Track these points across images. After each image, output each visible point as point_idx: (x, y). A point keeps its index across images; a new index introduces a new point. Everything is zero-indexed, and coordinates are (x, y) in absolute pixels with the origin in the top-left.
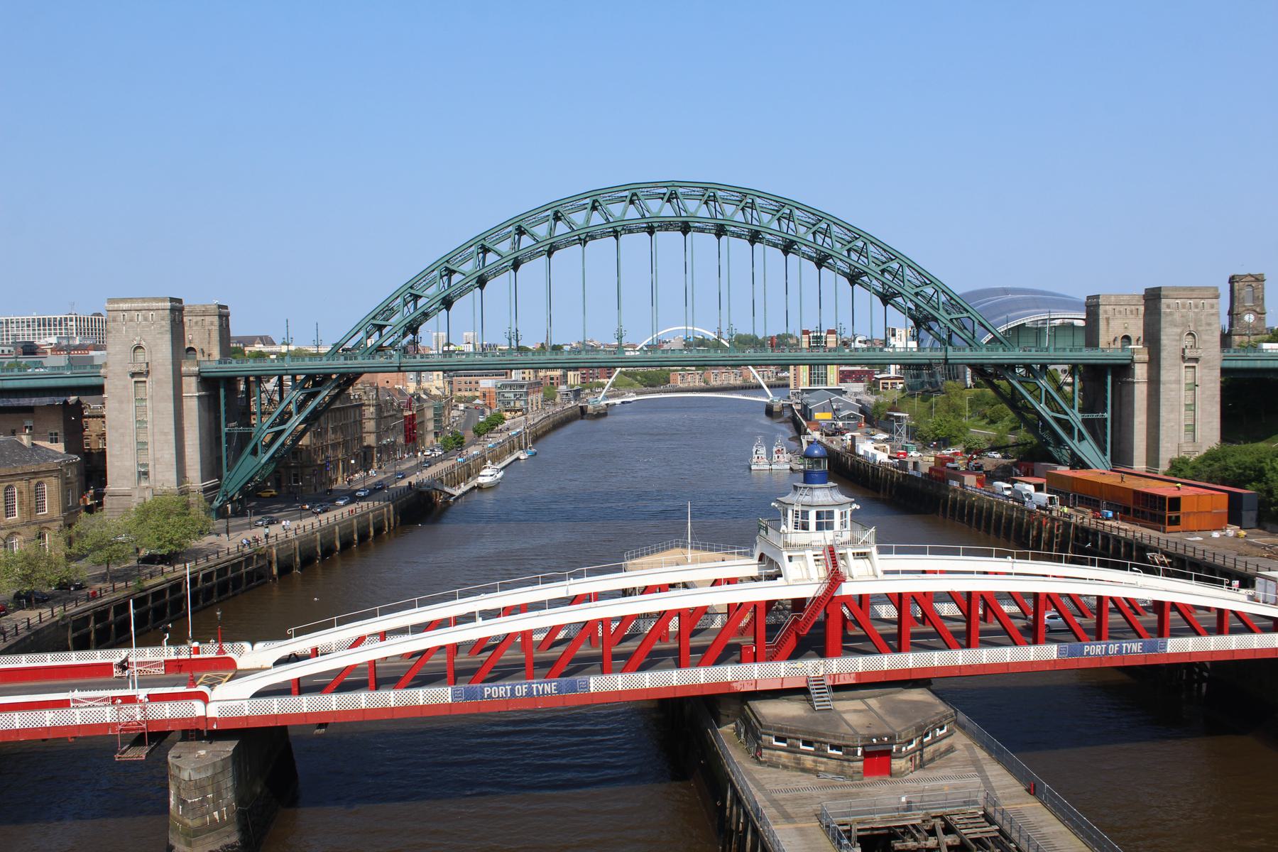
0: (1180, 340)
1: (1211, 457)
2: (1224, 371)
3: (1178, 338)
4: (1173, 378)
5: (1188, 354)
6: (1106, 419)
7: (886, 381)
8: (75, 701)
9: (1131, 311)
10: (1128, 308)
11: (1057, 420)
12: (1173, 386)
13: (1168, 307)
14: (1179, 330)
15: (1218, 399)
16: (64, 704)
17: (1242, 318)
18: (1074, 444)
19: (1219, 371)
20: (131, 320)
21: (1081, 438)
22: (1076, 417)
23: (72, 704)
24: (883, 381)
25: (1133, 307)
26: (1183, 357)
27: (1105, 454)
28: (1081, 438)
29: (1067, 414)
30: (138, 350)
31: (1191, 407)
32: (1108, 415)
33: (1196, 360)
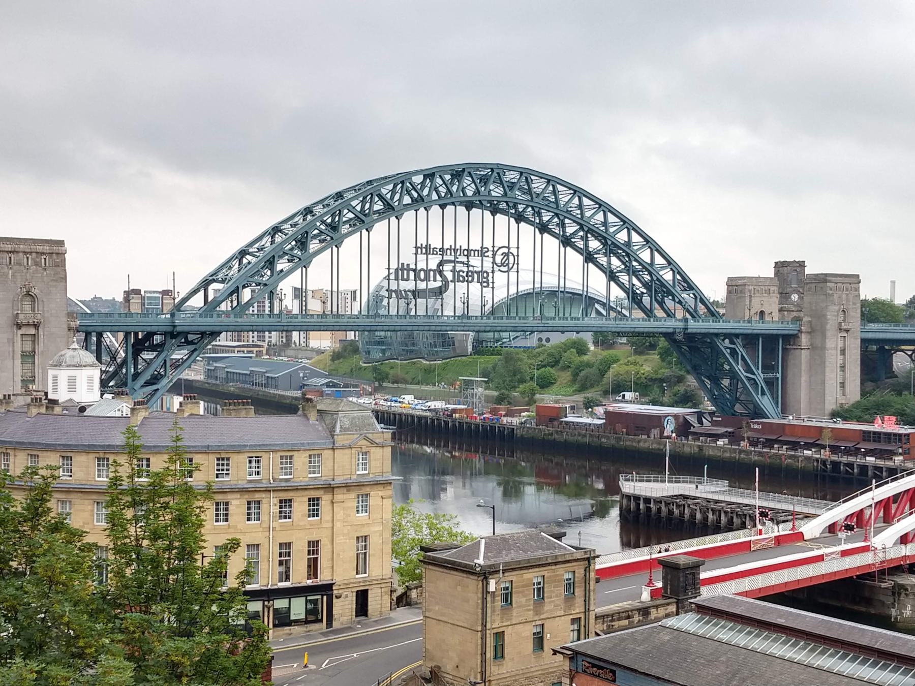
0: (838, 315)
1: (856, 405)
2: (865, 342)
3: (836, 314)
4: (833, 346)
5: (844, 326)
6: (778, 378)
7: (242, 349)
8: (827, 555)
9: (765, 291)
10: (762, 287)
11: (749, 379)
12: (834, 352)
13: (831, 289)
14: (836, 308)
15: (859, 362)
16: (820, 558)
17: (790, 297)
18: (758, 398)
19: (859, 340)
20: (20, 264)
21: (763, 393)
22: (760, 376)
23: (825, 558)
24: (239, 349)
25: (766, 288)
26: (840, 329)
27: (777, 407)
28: (763, 393)
29: (754, 374)
30: (28, 298)
31: (843, 368)
32: (779, 375)
33: (847, 331)
